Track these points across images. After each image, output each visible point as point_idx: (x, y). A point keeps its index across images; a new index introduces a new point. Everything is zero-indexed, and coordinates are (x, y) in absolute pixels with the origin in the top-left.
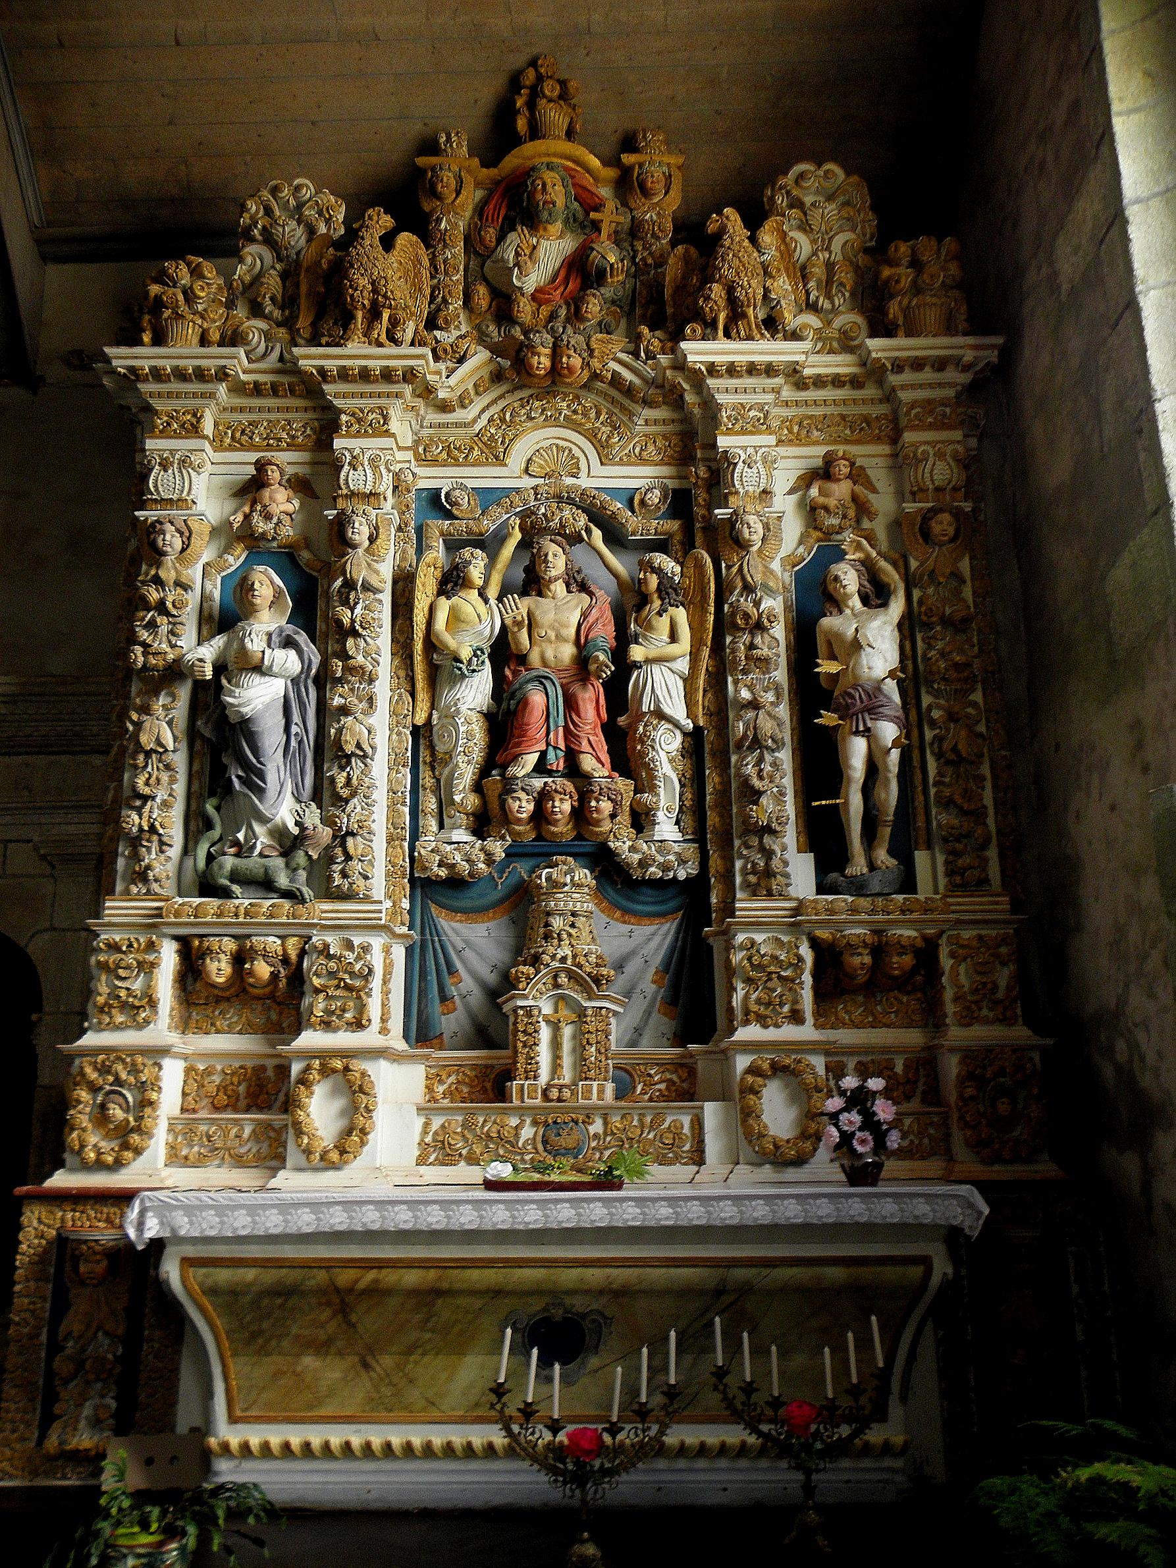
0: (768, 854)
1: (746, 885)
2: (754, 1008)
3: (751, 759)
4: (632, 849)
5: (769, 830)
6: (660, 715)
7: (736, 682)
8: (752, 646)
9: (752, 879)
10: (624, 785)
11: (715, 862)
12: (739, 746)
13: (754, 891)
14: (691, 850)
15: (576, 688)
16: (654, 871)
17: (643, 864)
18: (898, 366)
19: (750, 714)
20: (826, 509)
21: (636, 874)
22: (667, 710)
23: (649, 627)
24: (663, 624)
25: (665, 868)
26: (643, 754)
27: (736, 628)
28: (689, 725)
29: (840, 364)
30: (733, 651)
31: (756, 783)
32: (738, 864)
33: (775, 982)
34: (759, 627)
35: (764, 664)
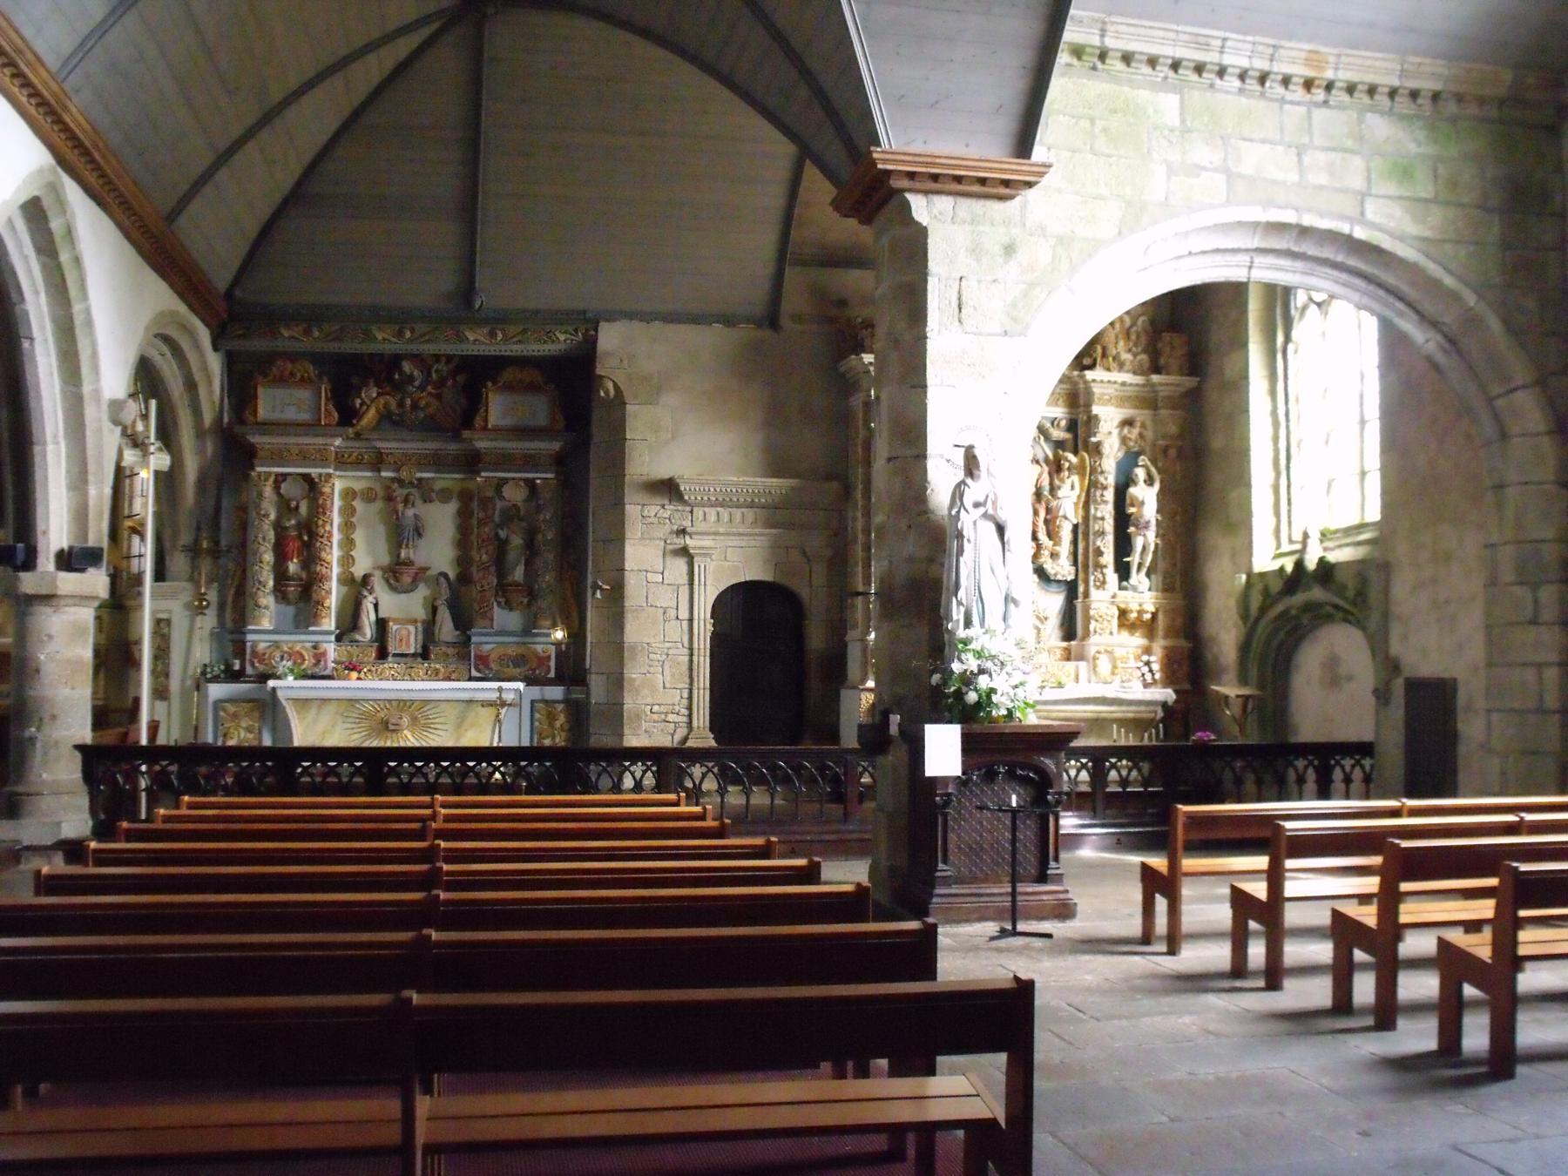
0: (1104, 575)
1: (1095, 585)
2: (1098, 630)
3: (1100, 539)
4: (1053, 568)
5: (1106, 567)
6: (1066, 518)
7: (1096, 509)
8: (1102, 495)
9: (1098, 584)
10: (1051, 543)
11: (1081, 576)
12: (1095, 533)
13: (1098, 588)
14: (1072, 569)
15: (1037, 506)
16: (1059, 577)
17: (1055, 575)
18: (1161, 384)
19: (1101, 522)
20: (1130, 439)
21: (1052, 578)
22: (1068, 516)
23: (1062, 481)
24: (1068, 482)
25: (1063, 576)
26: (1058, 532)
27: (1096, 487)
28: (1075, 522)
29: (1139, 380)
30: (1095, 496)
31: (1102, 549)
32: (1092, 578)
33: (1105, 622)
34: (1105, 488)
35: (1105, 502)
